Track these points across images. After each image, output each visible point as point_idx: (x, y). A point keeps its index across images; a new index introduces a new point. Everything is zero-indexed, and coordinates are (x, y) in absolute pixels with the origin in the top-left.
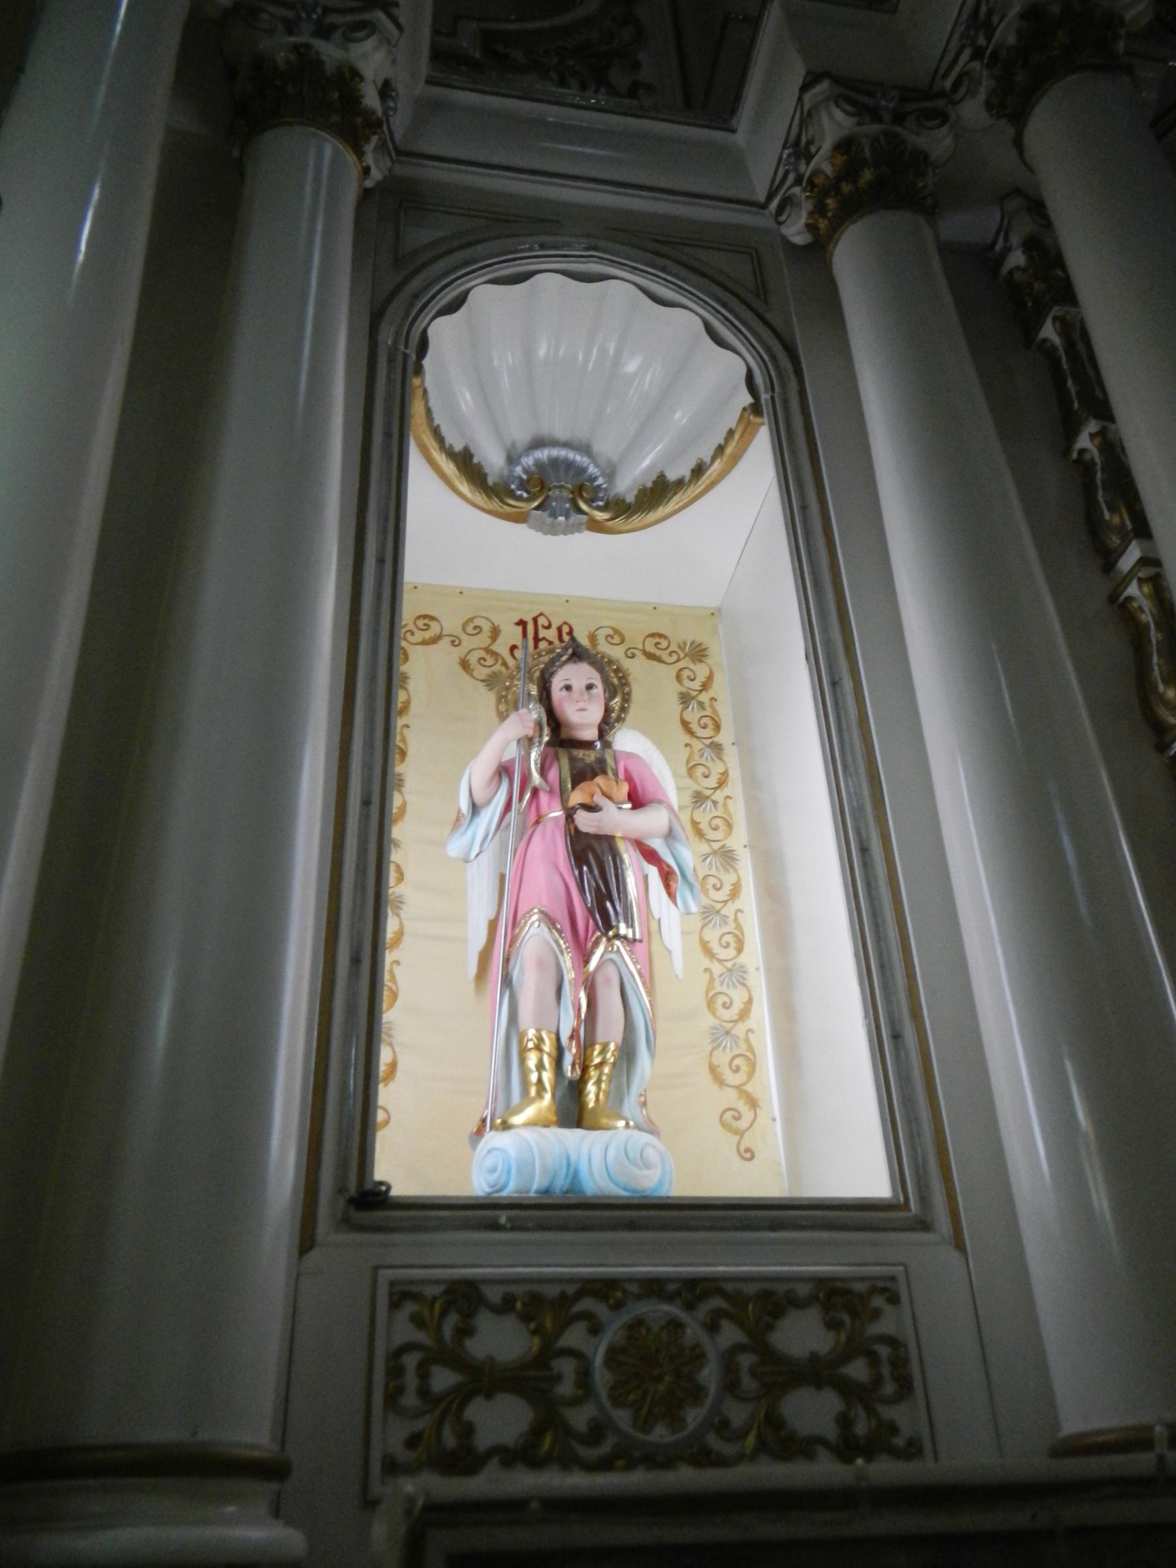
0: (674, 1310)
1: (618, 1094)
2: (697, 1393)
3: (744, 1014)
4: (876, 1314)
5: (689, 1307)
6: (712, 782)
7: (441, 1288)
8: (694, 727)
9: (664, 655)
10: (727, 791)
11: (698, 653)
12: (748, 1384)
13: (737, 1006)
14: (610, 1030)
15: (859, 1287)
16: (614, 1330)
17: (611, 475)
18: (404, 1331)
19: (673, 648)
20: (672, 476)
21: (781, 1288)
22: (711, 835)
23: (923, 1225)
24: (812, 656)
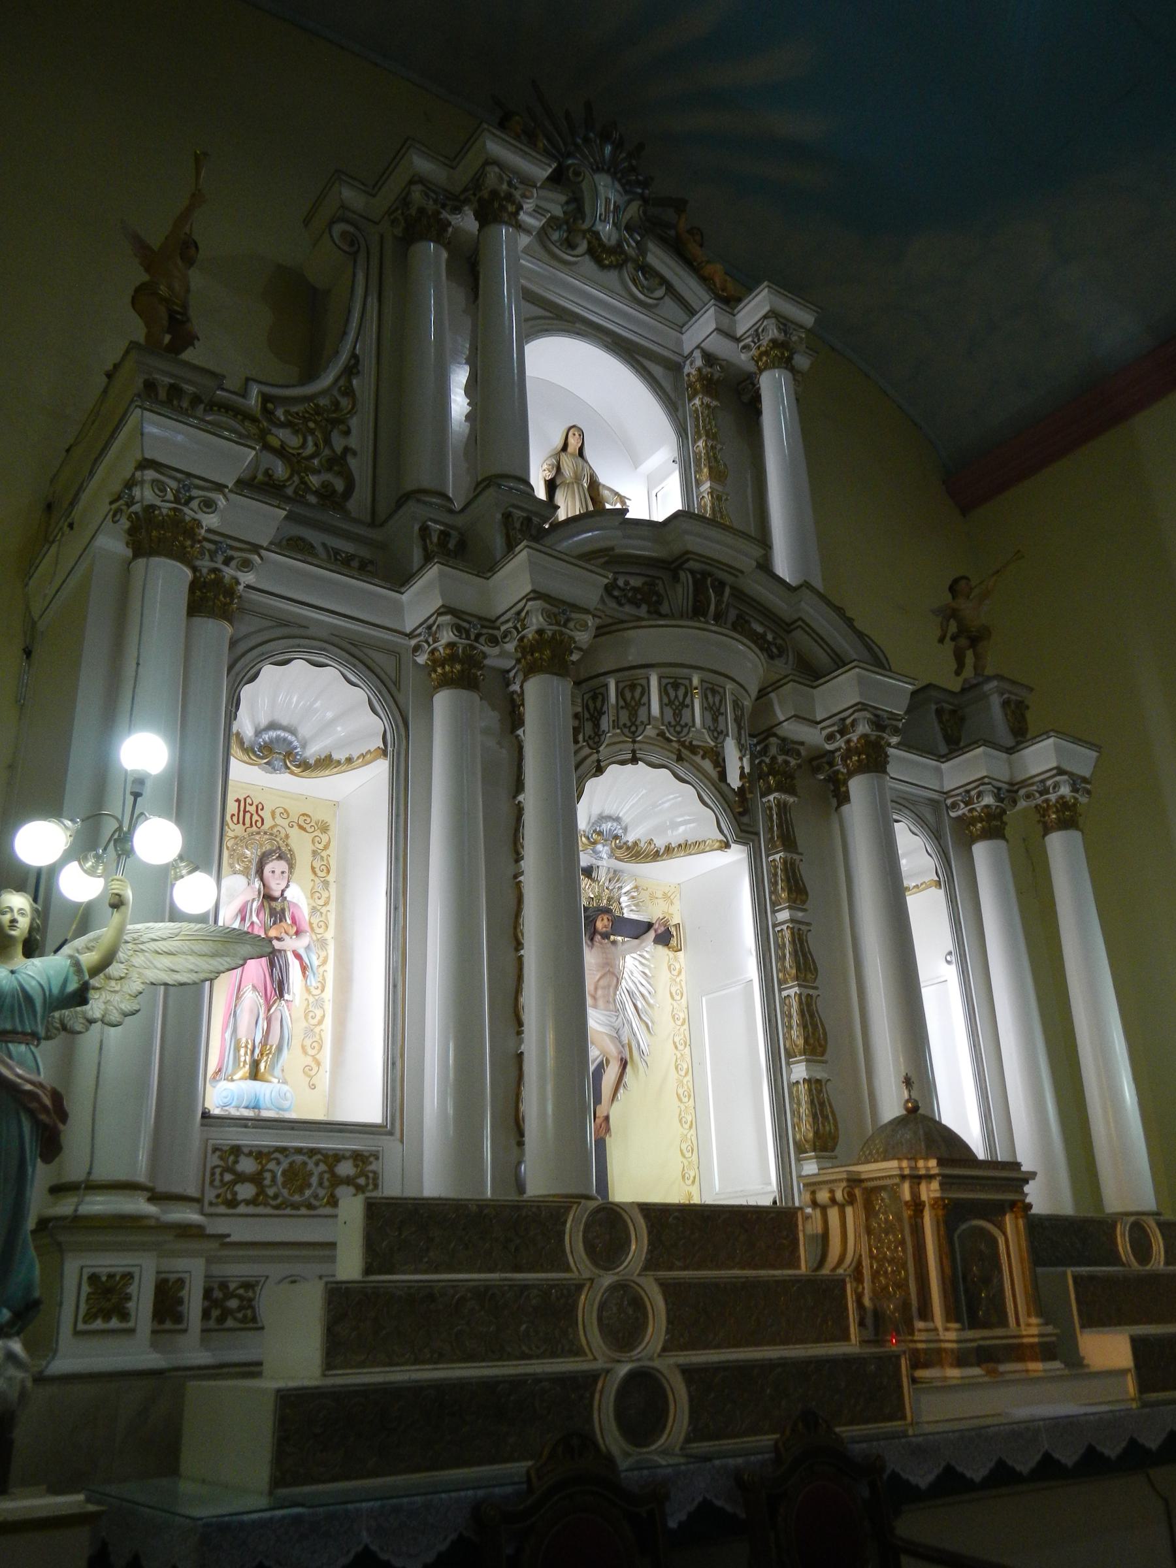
0: (305, 1158)
1: (272, 1067)
2: (309, 1186)
3: (320, 1022)
4: (371, 1163)
5: (310, 1157)
6: (321, 902)
7: (228, 1148)
8: (317, 870)
9: (307, 827)
10: (328, 908)
11: (325, 828)
12: (326, 1183)
13: (318, 1018)
14: (274, 1040)
15: (366, 1154)
16: (285, 1164)
17: (304, 746)
18: (214, 1160)
19: (312, 824)
20: (336, 756)
21: (341, 1153)
22: (318, 930)
23: (391, 1133)
24: (389, 893)
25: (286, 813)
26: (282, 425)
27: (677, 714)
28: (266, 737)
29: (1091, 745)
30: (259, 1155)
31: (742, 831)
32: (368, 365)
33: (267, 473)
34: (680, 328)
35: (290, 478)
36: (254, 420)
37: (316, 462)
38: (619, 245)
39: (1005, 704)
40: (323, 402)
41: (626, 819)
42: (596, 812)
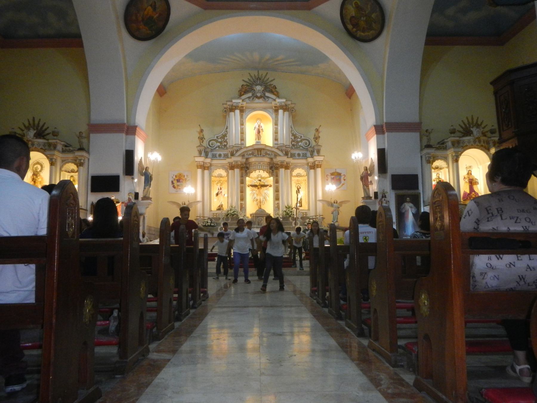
25: (224, 180)
26: (219, 139)
27: (255, 167)
28: (219, 175)
29: (322, 156)
30: (216, 214)
31: (272, 175)
32: (228, 128)
33: (218, 145)
34: (271, 103)
35: (220, 145)
36: (216, 140)
37: (223, 142)
38: (261, 96)
39: (316, 149)
40: (224, 134)
41: (262, 175)
42: (258, 174)
